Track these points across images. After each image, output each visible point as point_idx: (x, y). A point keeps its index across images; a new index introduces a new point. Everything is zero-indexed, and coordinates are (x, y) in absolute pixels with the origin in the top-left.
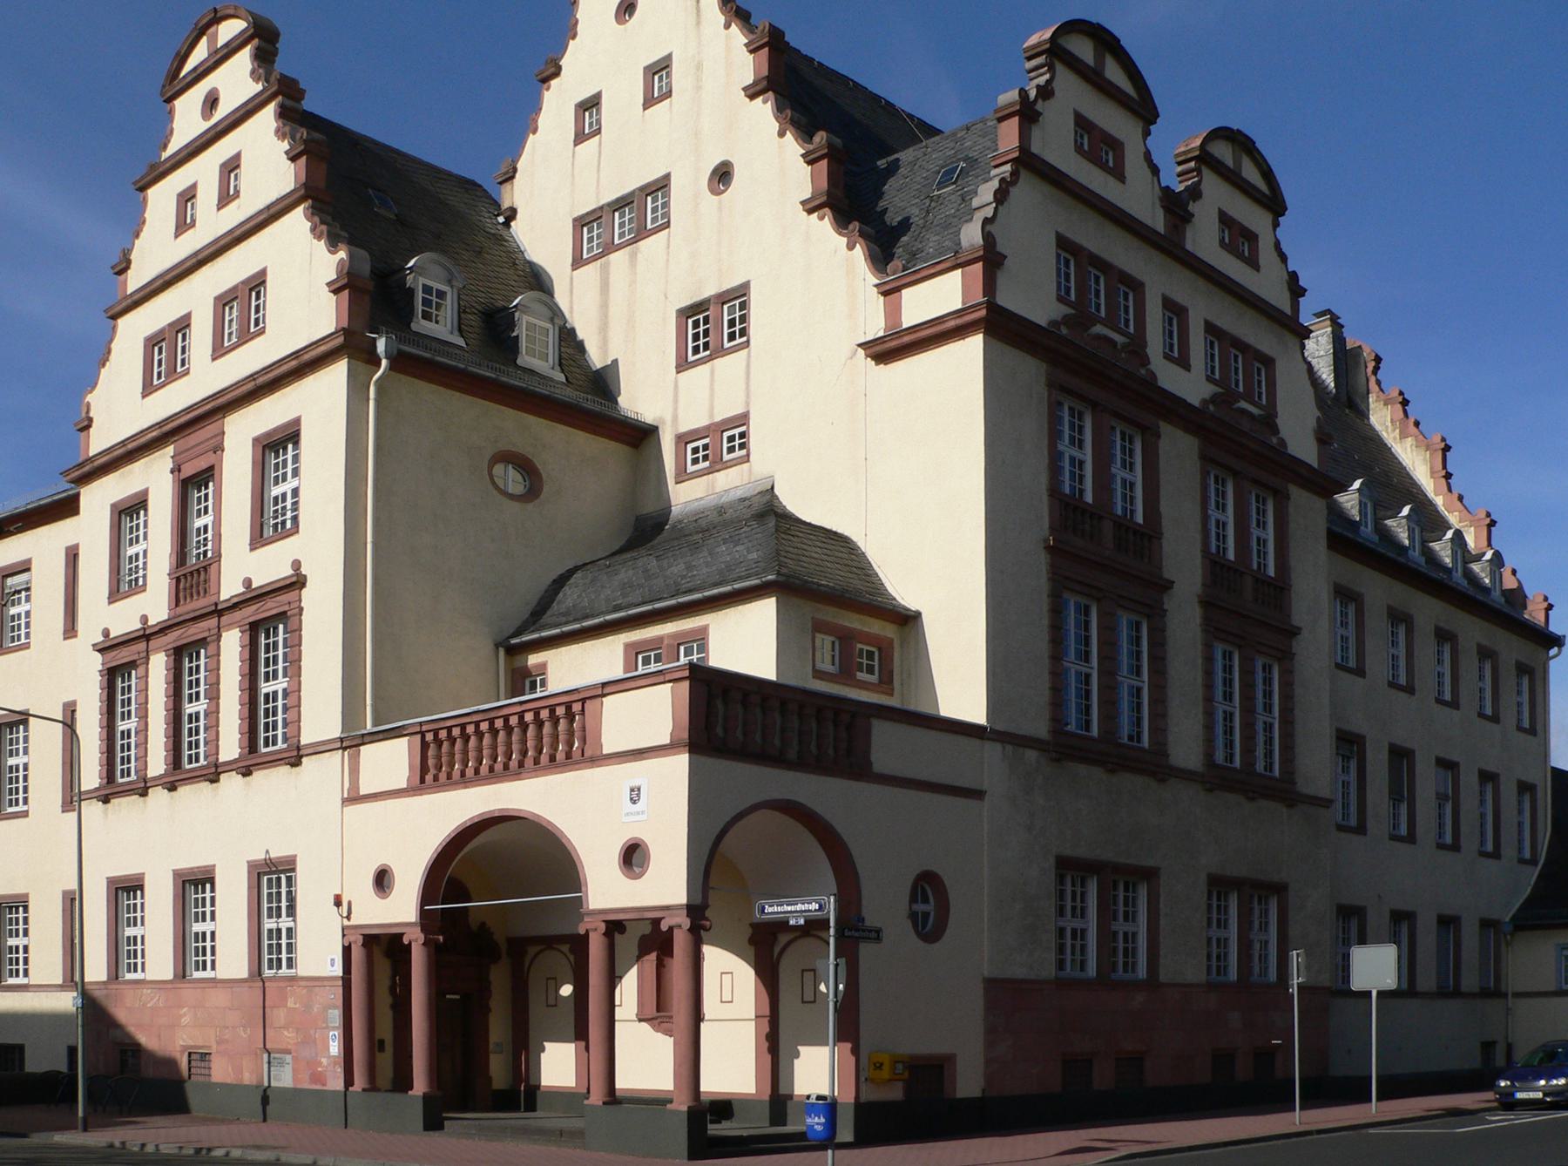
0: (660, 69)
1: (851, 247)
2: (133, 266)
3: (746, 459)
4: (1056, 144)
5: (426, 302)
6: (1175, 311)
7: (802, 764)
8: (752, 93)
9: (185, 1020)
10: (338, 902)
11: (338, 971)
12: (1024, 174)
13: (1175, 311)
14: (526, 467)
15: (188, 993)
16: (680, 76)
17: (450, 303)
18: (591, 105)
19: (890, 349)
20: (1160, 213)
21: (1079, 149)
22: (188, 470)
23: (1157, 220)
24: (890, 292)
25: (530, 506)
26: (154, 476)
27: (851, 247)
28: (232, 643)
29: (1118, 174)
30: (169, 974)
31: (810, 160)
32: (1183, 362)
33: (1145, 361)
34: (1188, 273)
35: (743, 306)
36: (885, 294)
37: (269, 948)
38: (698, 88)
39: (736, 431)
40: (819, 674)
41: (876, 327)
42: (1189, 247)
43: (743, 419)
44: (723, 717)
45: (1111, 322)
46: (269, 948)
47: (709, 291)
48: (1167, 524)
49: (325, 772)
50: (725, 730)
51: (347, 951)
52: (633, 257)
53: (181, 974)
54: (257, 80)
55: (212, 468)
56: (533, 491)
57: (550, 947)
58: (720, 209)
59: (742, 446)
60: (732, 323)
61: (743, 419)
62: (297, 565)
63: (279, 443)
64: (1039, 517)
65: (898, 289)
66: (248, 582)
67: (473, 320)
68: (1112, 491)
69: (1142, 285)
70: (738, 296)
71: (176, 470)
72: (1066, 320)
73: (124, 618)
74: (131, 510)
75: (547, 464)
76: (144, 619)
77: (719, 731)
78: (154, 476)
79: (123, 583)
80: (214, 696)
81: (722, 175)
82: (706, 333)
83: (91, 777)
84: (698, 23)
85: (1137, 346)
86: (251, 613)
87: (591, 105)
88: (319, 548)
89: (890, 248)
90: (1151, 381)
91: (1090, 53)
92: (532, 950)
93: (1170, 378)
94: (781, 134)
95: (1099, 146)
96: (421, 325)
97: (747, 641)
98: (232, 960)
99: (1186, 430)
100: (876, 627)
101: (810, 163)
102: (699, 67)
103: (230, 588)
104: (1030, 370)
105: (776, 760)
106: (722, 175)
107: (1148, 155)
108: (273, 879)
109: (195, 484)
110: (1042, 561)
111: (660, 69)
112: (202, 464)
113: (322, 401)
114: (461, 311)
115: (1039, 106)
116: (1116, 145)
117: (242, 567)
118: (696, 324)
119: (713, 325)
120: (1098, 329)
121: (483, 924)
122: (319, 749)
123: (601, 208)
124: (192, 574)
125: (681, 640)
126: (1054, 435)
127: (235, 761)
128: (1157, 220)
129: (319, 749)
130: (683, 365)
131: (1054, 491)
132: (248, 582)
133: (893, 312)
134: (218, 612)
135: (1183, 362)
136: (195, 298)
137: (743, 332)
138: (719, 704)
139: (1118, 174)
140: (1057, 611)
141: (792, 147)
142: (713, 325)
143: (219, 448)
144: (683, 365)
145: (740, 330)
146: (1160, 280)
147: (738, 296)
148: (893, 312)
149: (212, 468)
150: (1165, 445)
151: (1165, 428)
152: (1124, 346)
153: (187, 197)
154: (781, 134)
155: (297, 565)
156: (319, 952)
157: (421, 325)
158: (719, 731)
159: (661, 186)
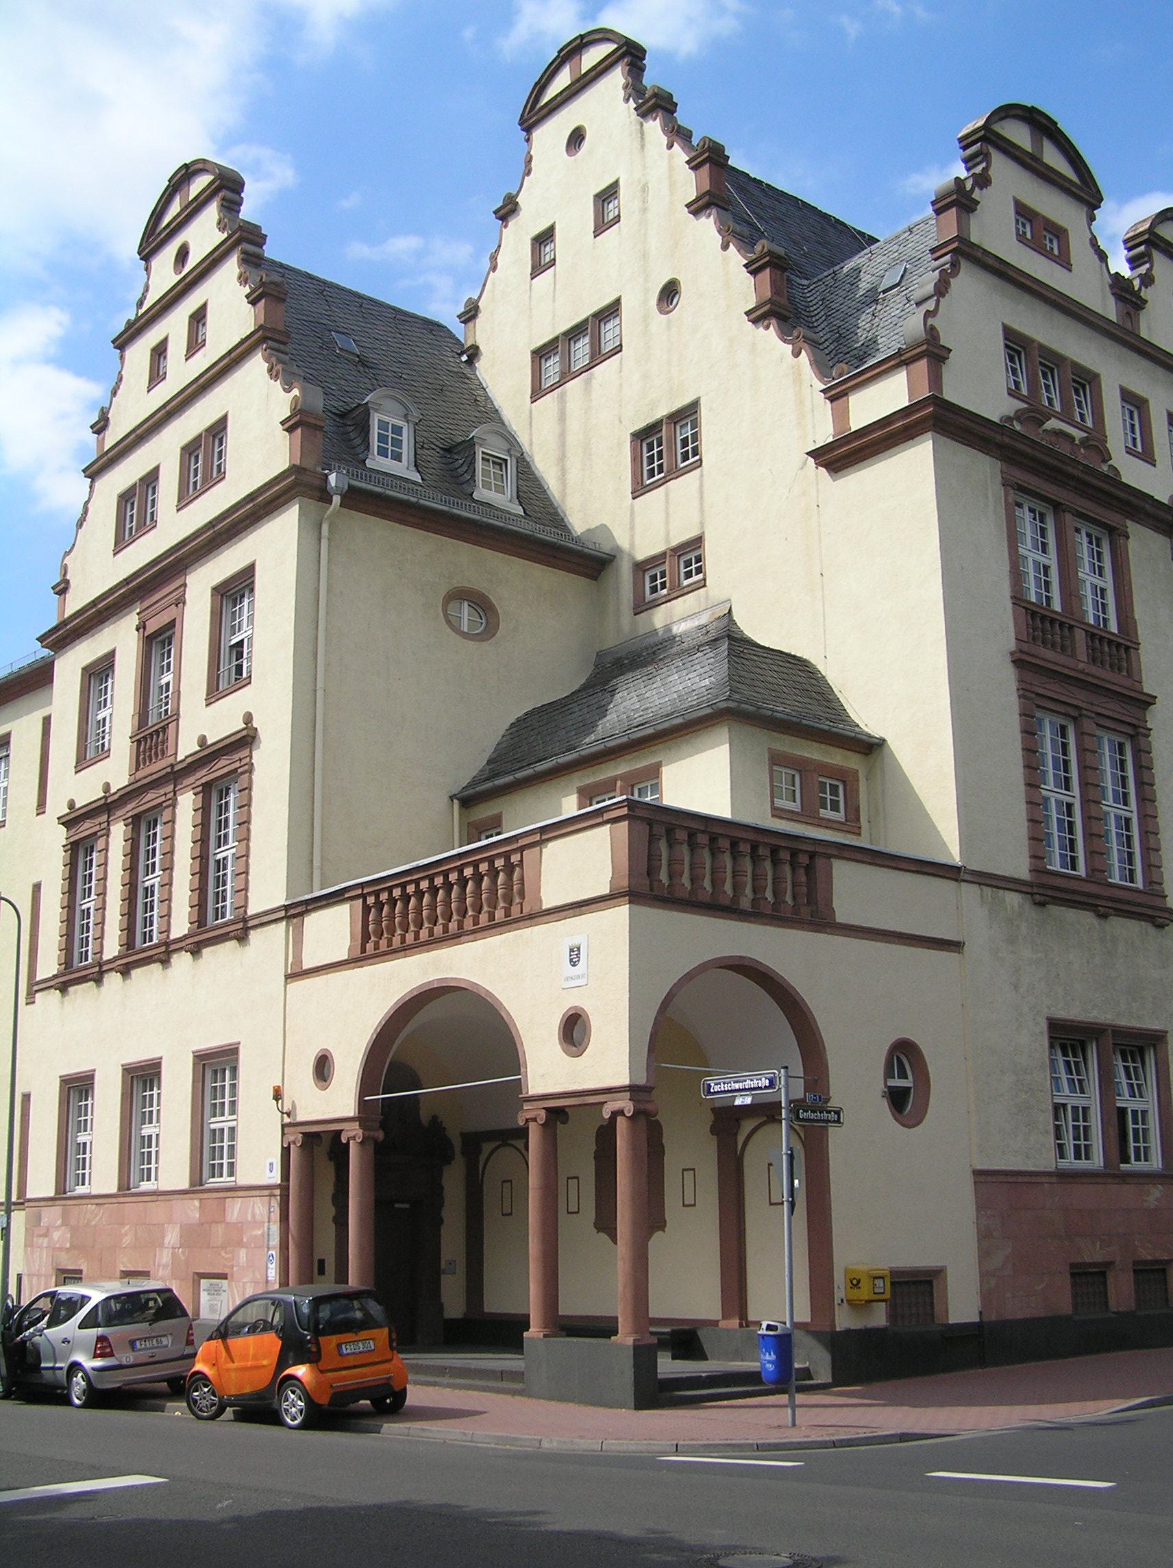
0: (608, 195)
1: (796, 354)
2: (110, 427)
3: (703, 584)
4: (995, 230)
5: (382, 439)
6: (1134, 403)
7: (754, 915)
8: (697, 208)
9: (127, 1240)
10: (278, 1095)
11: (276, 1178)
12: (964, 264)
13: (1134, 403)
14: (482, 604)
15: (131, 1208)
16: (626, 201)
17: (406, 437)
18: (544, 238)
19: (842, 455)
20: (1111, 301)
21: (1021, 238)
22: (152, 626)
23: (1109, 309)
24: (836, 395)
25: (485, 644)
26: (122, 638)
27: (796, 354)
28: (187, 804)
29: (1064, 261)
30: (113, 1188)
31: (754, 269)
32: (1147, 456)
33: (1105, 456)
34: (1145, 364)
35: (695, 424)
36: (832, 399)
37: (210, 1150)
38: (644, 210)
39: (692, 556)
40: (777, 812)
41: (825, 434)
42: (1144, 334)
43: (698, 542)
44: (672, 863)
45: (1066, 417)
46: (210, 1150)
47: (662, 412)
48: (1143, 633)
49: (269, 943)
50: (670, 877)
51: (286, 1152)
52: (588, 382)
53: (125, 1185)
54: (222, 229)
55: (172, 624)
56: (490, 631)
57: (505, 1144)
58: (669, 327)
59: (699, 570)
60: (685, 442)
61: (698, 542)
62: (248, 718)
63: (235, 590)
64: (1003, 631)
65: (844, 394)
66: (202, 741)
67: (433, 456)
68: (1080, 598)
69: (1097, 376)
70: (688, 414)
71: (141, 627)
72: (1019, 416)
73: (87, 789)
74: (99, 672)
75: (505, 600)
76: (107, 787)
77: (663, 876)
78: (122, 638)
79: (89, 752)
80: (168, 868)
81: (670, 292)
82: (660, 457)
83: (49, 966)
84: (643, 147)
85: (1096, 444)
86: (203, 776)
87: (544, 238)
88: (268, 698)
89: (843, 361)
90: (1113, 479)
91: (1025, 141)
92: (487, 1148)
93: (1133, 474)
94: (725, 247)
95: (1042, 233)
96: (376, 462)
97: (702, 782)
98: (173, 1167)
99: (1156, 529)
100: (837, 758)
101: (754, 273)
102: (645, 189)
103: (186, 747)
104: (984, 469)
105: (729, 910)
106: (670, 292)
107: (1094, 242)
108: (217, 1066)
109: (159, 642)
110: (1008, 677)
111: (608, 195)
112: (164, 619)
113: (276, 546)
114: (418, 447)
115: (976, 195)
116: (1060, 233)
117: (200, 723)
118: (650, 448)
119: (665, 446)
120: (1053, 424)
121: (435, 1118)
122: (267, 919)
123: (556, 339)
124: (152, 737)
125: (631, 780)
126: (1013, 539)
127: (185, 937)
128: (1109, 309)
129: (267, 919)
130: (639, 490)
131: (1018, 599)
132: (202, 741)
133: (841, 417)
134: (176, 776)
135: (1147, 456)
136: (164, 452)
137: (696, 452)
138: (663, 845)
139: (1064, 261)
140: (1030, 732)
141: (735, 258)
142: (665, 446)
143: (180, 602)
144: (639, 490)
145: (691, 452)
146: (1115, 372)
147: (688, 414)
148: (841, 417)
149: (172, 624)
150: (1132, 545)
151: (1132, 527)
152: (1083, 442)
153: (160, 351)
154: (725, 247)
155: (248, 718)
156: (259, 1157)
157: (376, 462)
158: (663, 876)
159: (612, 310)
